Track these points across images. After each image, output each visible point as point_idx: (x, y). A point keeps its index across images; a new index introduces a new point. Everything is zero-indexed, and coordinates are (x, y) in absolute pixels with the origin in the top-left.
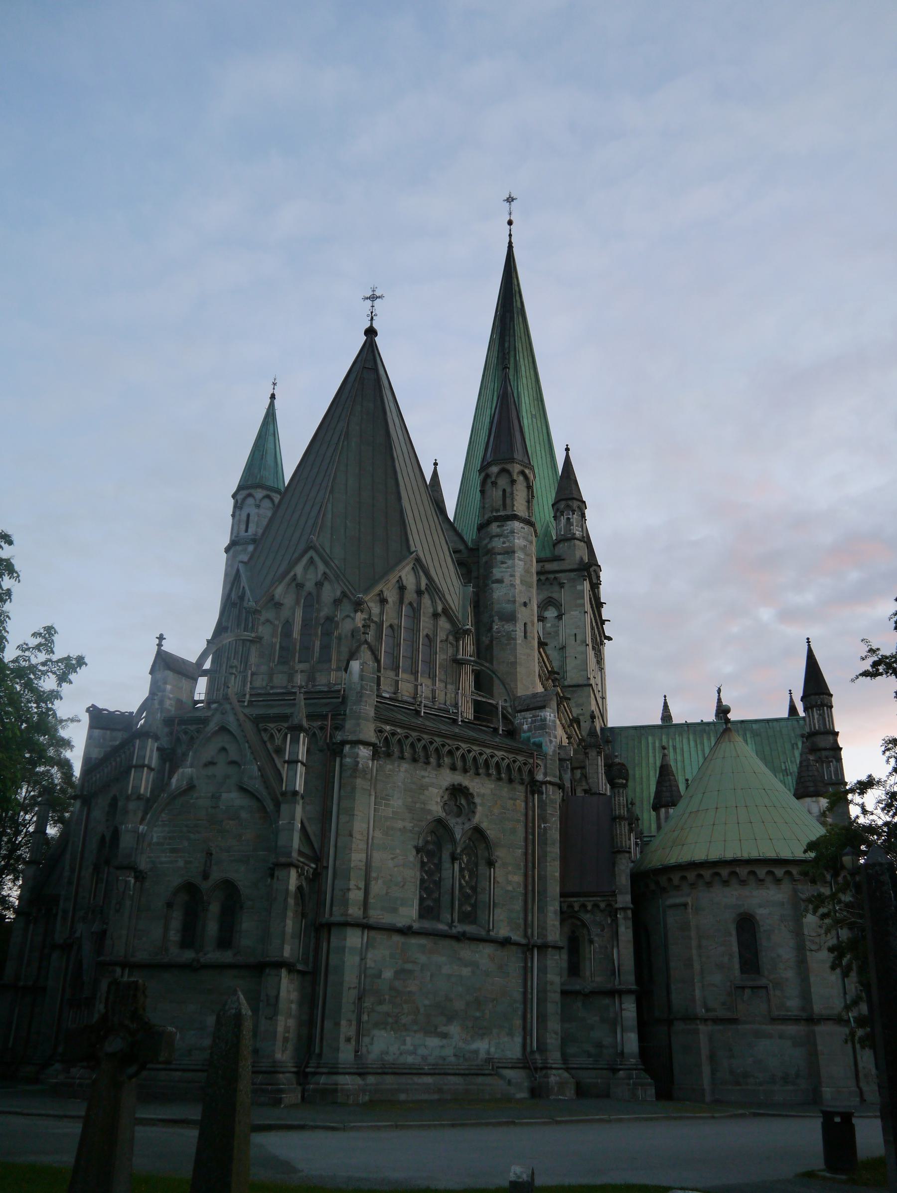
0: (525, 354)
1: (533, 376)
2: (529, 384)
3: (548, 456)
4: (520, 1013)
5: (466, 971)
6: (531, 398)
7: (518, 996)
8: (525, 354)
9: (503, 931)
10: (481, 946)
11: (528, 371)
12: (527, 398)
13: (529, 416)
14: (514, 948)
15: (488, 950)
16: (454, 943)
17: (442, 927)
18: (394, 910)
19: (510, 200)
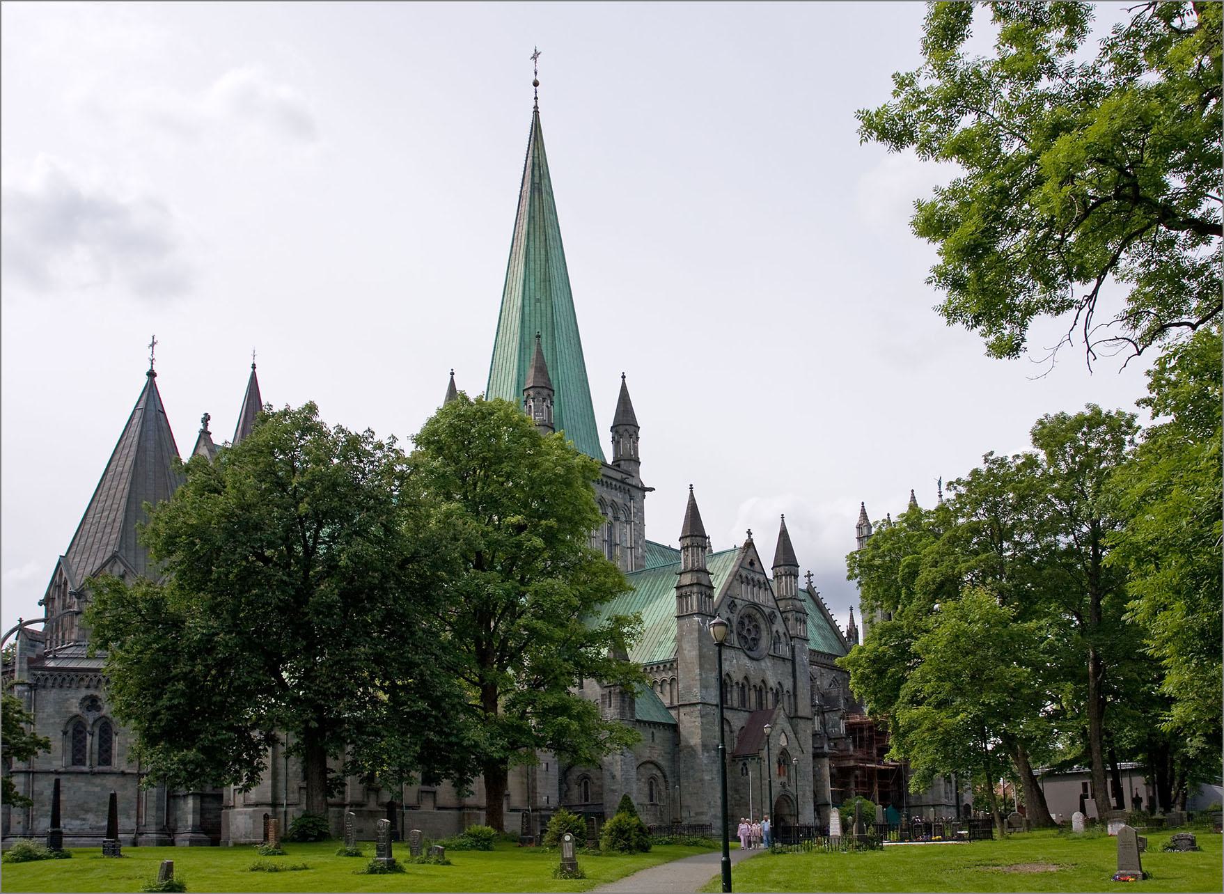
0: (537, 234)
1: (543, 257)
2: (538, 266)
3: (550, 338)
4: (135, 807)
5: (97, 789)
6: (538, 281)
7: (135, 800)
8: (537, 234)
9: (124, 767)
10: (107, 776)
11: (537, 253)
12: (532, 284)
13: (533, 301)
14: (131, 776)
15: (113, 778)
16: (89, 776)
17: (85, 769)
18: (50, 763)
19: (535, 56)
